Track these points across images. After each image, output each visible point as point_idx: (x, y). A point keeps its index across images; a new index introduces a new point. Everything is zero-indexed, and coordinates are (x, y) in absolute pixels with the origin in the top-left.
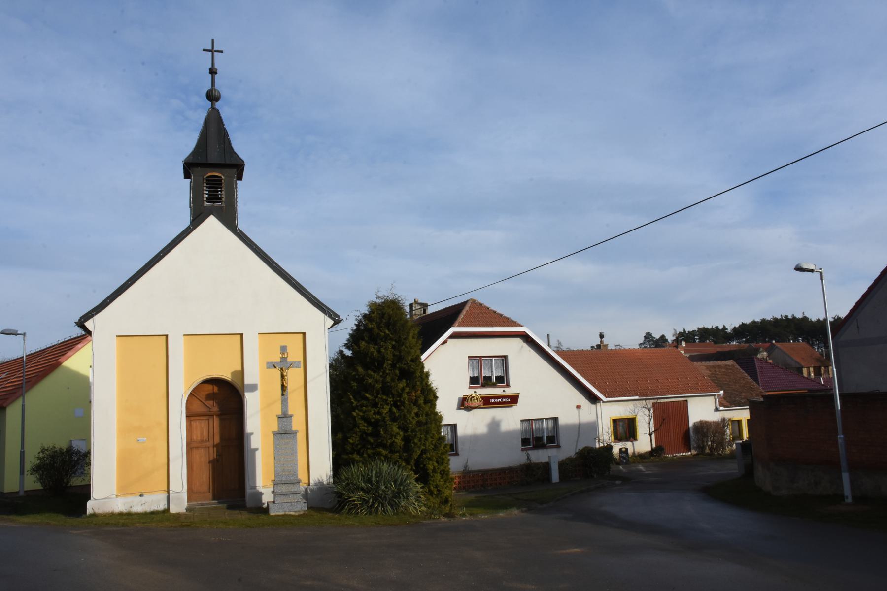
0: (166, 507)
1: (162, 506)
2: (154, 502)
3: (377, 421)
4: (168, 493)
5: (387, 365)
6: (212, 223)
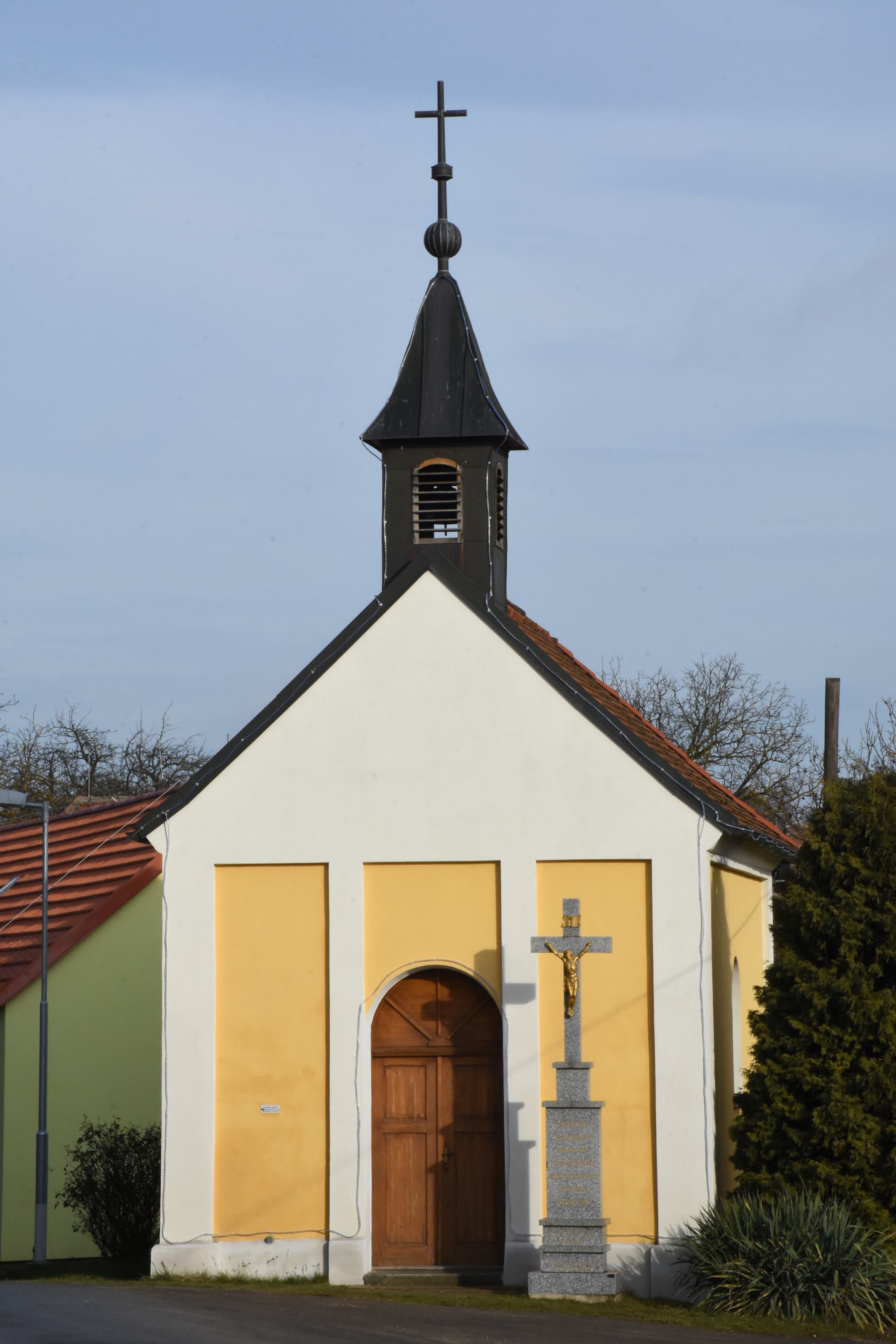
0: (321, 1271)
1: (310, 1268)
2: (289, 1258)
3: (816, 1090)
4: (328, 1239)
5: (847, 950)
6: (428, 590)
